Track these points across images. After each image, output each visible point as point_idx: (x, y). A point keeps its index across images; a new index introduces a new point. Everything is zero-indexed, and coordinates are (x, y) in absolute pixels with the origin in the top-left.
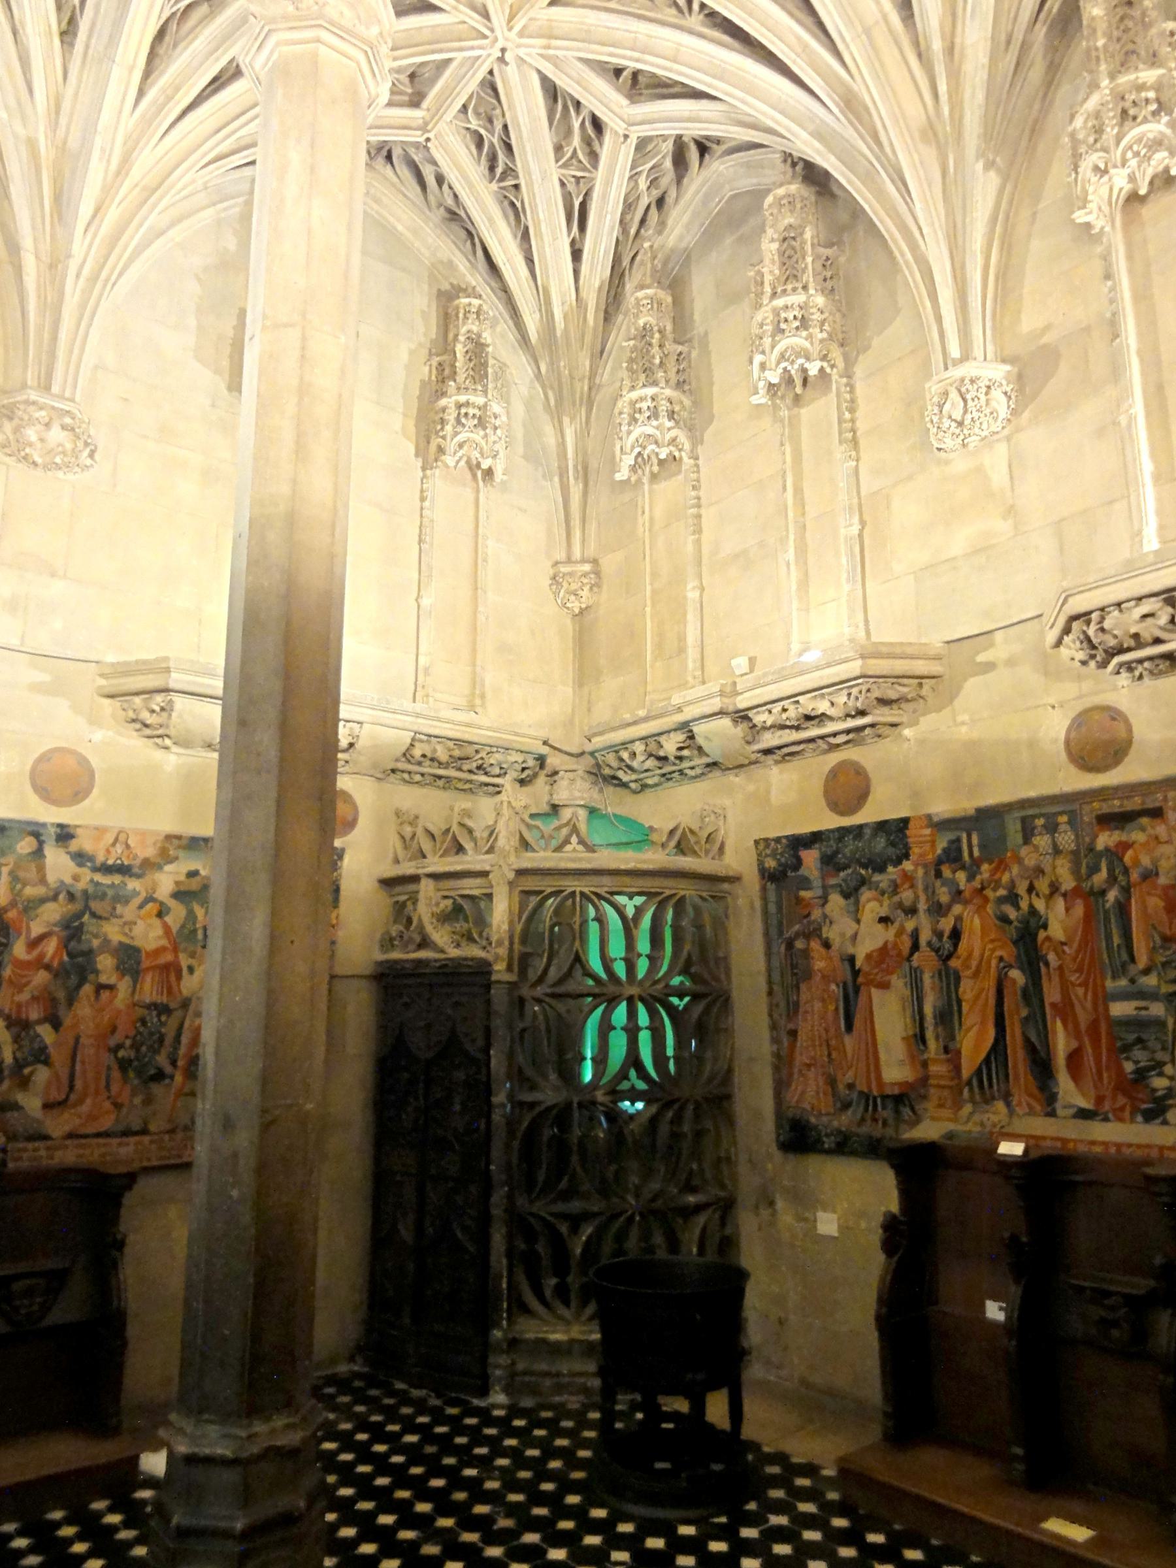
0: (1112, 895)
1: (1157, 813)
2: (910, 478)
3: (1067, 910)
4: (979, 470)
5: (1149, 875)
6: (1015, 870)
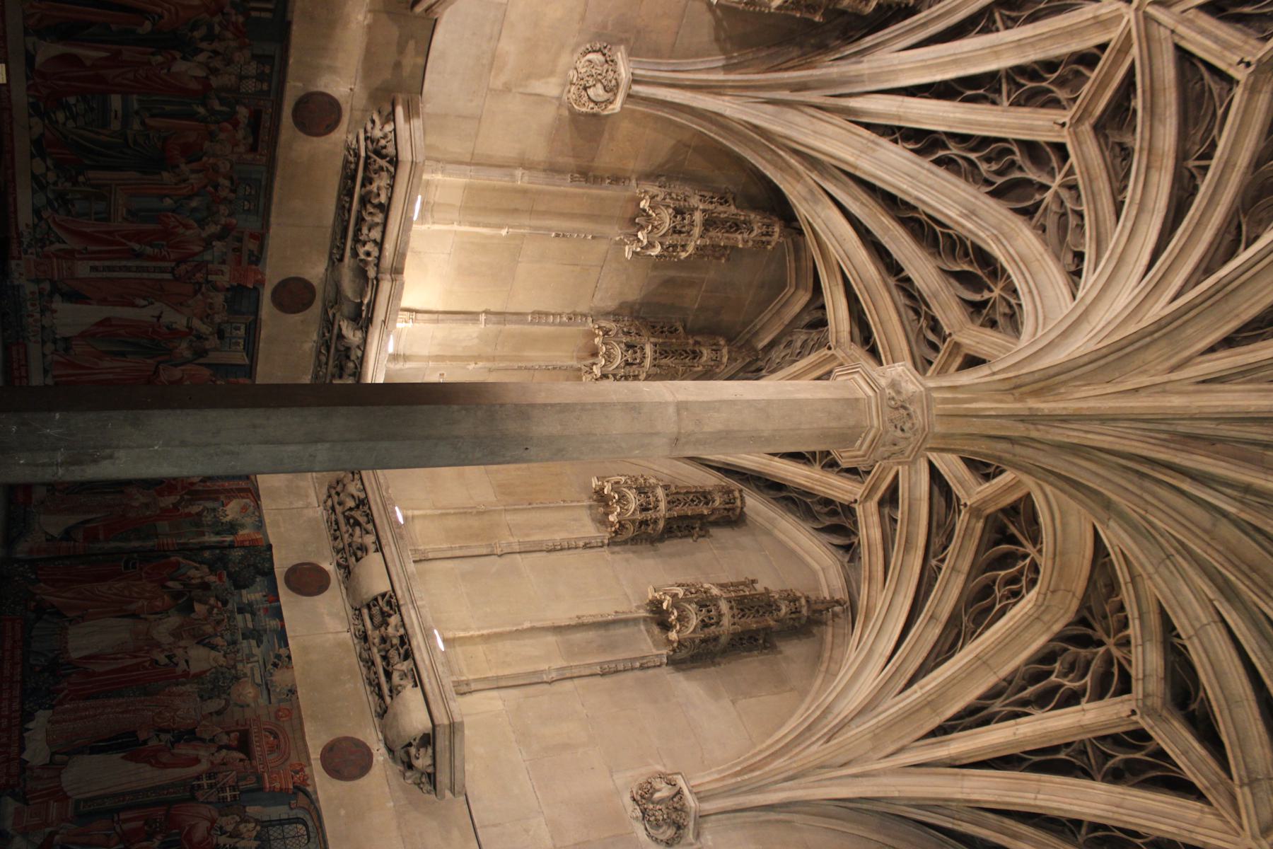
0: (201, 110)
1: (253, 148)
2: (583, 19)
3: (196, 78)
4: (552, 73)
5: (211, 136)
6: (233, 44)
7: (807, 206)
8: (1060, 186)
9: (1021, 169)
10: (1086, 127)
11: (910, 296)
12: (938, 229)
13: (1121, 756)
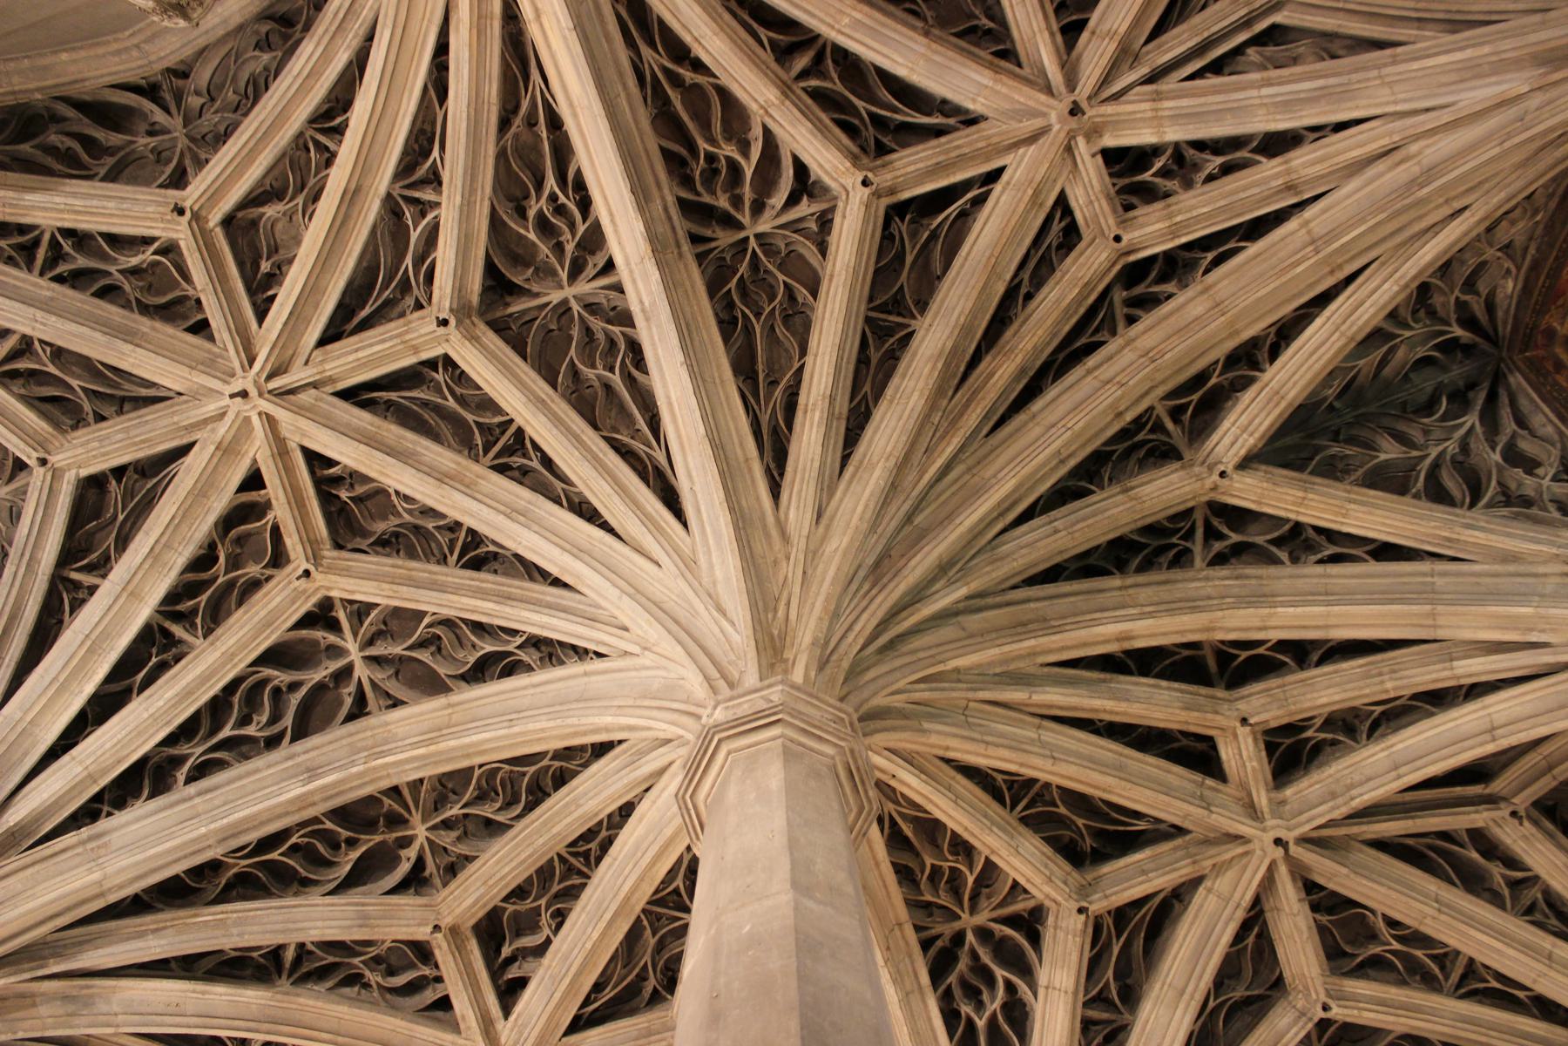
7: (83, 1020)
8: (361, 649)
9: (294, 686)
10: (329, 553)
11: (321, 974)
12: (274, 855)
13: (1110, 973)
